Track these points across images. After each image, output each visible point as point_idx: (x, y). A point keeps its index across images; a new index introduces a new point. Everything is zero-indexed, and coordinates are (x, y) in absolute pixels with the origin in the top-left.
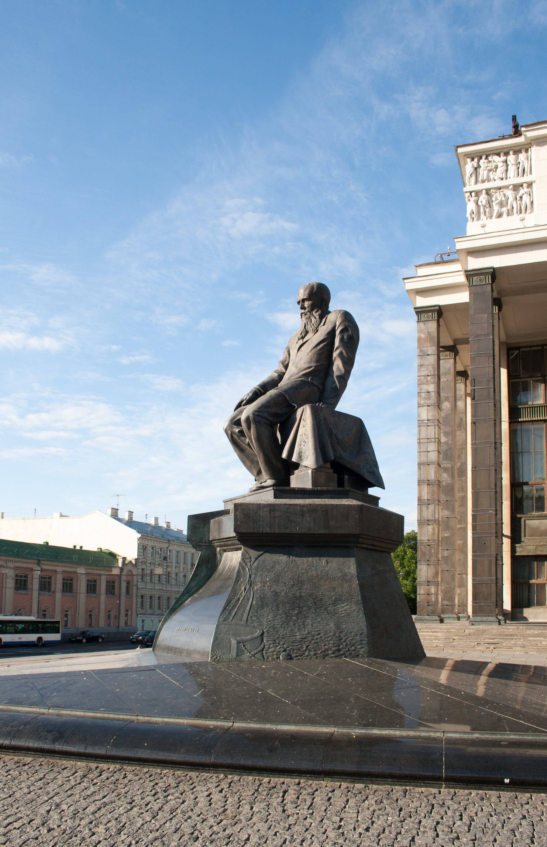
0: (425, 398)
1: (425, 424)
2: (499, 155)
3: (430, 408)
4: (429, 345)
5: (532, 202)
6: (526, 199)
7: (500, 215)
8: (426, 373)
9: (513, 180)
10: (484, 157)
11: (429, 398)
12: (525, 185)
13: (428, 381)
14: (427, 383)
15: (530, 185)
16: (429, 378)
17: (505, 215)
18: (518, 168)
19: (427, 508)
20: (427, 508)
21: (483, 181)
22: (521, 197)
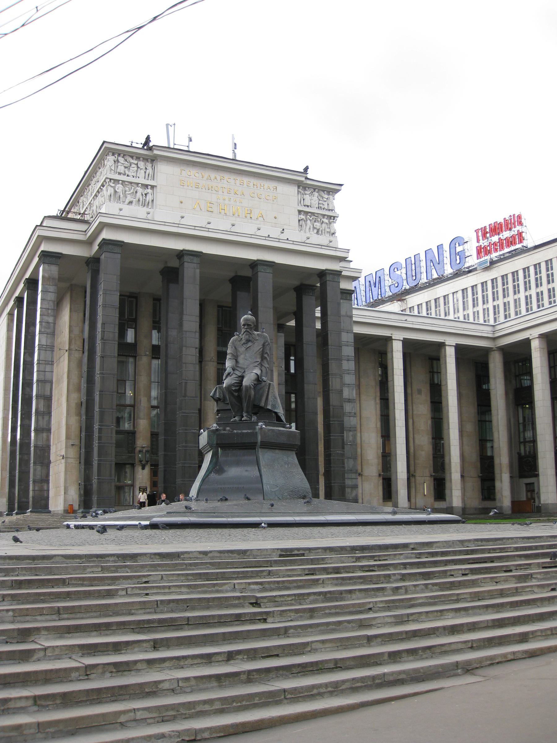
0: (45, 328)
1: (44, 349)
2: (132, 157)
3: (49, 336)
4: (51, 284)
5: (153, 201)
6: (149, 198)
7: (131, 203)
8: (47, 306)
10: (122, 155)
11: (49, 328)
12: (149, 187)
13: (48, 313)
14: (48, 315)
15: (153, 187)
16: (50, 311)
17: (134, 204)
18: (145, 172)
19: (43, 418)
20: (43, 418)
21: (120, 174)
22: (146, 194)
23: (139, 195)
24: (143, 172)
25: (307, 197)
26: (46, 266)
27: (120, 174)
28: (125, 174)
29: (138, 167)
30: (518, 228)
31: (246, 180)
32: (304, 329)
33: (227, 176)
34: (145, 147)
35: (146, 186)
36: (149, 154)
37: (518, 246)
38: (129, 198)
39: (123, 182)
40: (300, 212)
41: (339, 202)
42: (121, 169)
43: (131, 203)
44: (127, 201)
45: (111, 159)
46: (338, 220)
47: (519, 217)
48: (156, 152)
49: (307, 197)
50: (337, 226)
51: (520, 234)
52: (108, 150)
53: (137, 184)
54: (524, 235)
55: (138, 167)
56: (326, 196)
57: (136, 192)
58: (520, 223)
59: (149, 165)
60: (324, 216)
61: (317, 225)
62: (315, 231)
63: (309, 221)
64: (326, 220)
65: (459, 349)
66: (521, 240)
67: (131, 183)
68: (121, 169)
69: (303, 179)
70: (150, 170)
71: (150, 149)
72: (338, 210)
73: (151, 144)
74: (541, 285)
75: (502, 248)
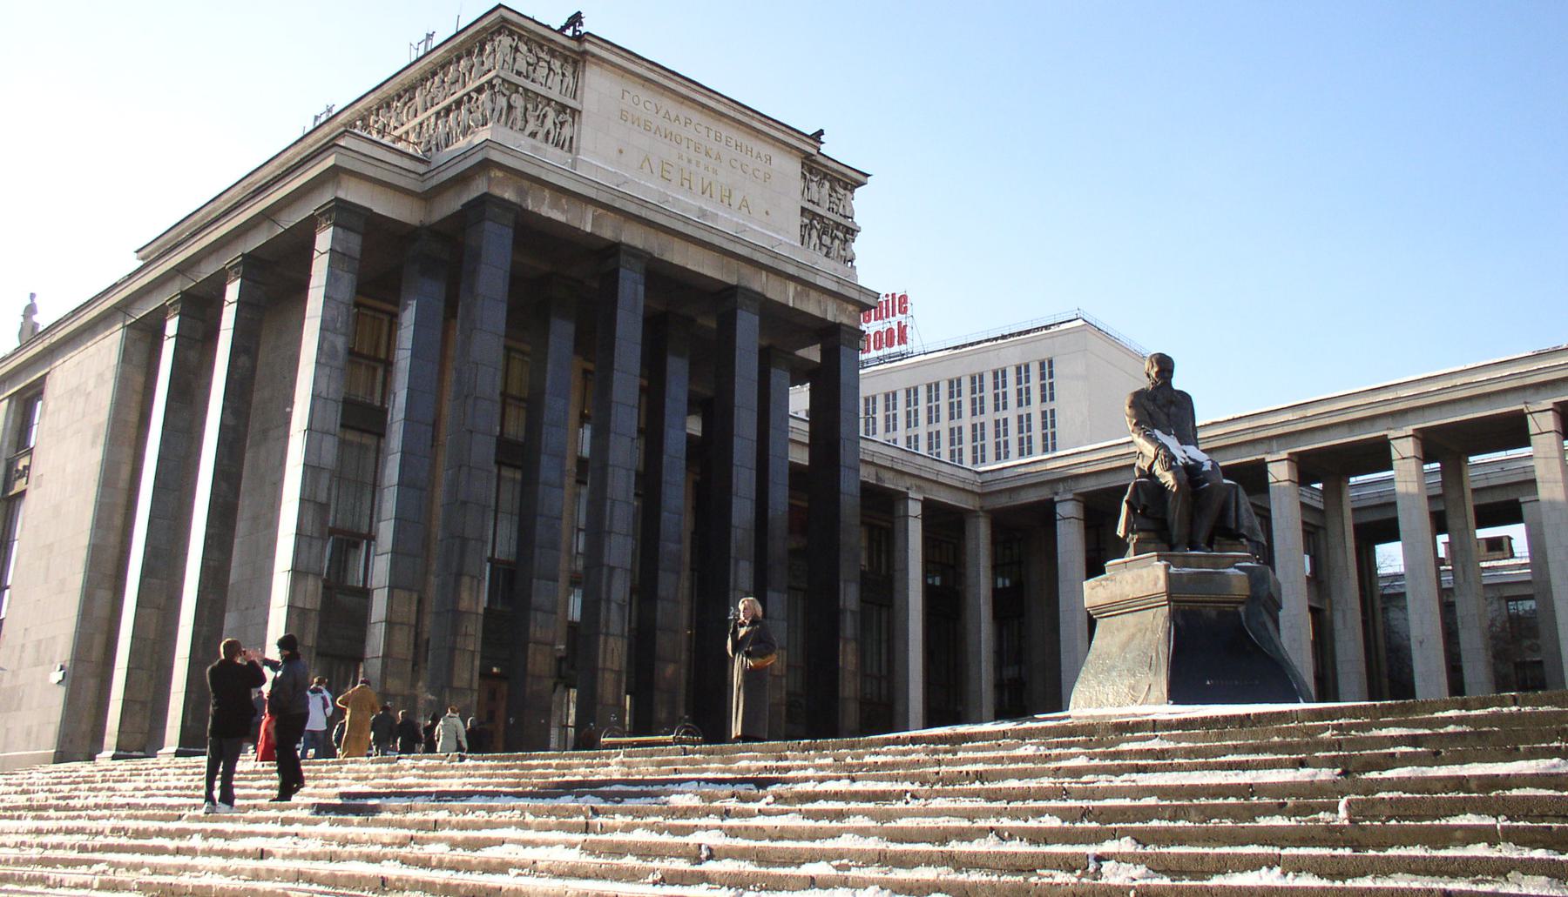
2: (541, 46)
6: (567, 131)
9: (554, 94)
14: (335, 331)
21: (519, 73)
22: (562, 124)
23: (549, 123)
24: (559, 78)
25: (814, 186)
26: (340, 231)
27: (519, 73)
28: (527, 77)
29: (550, 69)
30: (899, 316)
31: (726, 131)
32: (771, 432)
33: (696, 116)
34: (569, 32)
35: (563, 108)
36: (574, 48)
37: (896, 349)
38: (531, 127)
39: (526, 90)
40: (803, 210)
41: (862, 204)
42: (521, 65)
43: (533, 135)
44: (527, 132)
45: (506, 41)
46: (859, 237)
47: (904, 299)
48: (588, 46)
49: (814, 186)
50: (858, 246)
51: (902, 330)
52: (501, 24)
53: (549, 100)
54: (908, 330)
55: (550, 69)
56: (841, 191)
57: (545, 116)
58: (904, 311)
59: (569, 71)
60: (838, 225)
61: (826, 240)
62: (825, 250)
63: (814, 233)
64: (841, 235)
65: (928, 505)
66: (903, 339)
67: (537, 95)
68: (521, 65)
69: (814, 151)
70: (569, 80)
71: (579, 38)
72: (859, 220)
73: (583, 30)
74: (937, 420)
75: (891, 345)
